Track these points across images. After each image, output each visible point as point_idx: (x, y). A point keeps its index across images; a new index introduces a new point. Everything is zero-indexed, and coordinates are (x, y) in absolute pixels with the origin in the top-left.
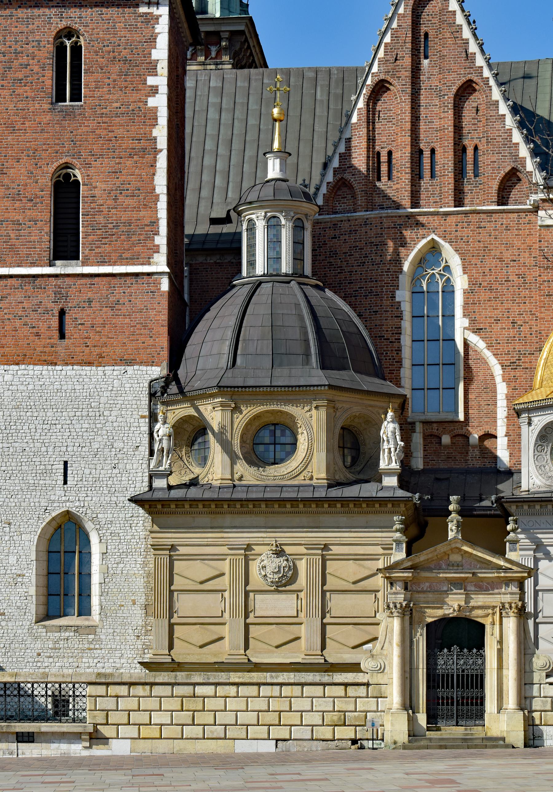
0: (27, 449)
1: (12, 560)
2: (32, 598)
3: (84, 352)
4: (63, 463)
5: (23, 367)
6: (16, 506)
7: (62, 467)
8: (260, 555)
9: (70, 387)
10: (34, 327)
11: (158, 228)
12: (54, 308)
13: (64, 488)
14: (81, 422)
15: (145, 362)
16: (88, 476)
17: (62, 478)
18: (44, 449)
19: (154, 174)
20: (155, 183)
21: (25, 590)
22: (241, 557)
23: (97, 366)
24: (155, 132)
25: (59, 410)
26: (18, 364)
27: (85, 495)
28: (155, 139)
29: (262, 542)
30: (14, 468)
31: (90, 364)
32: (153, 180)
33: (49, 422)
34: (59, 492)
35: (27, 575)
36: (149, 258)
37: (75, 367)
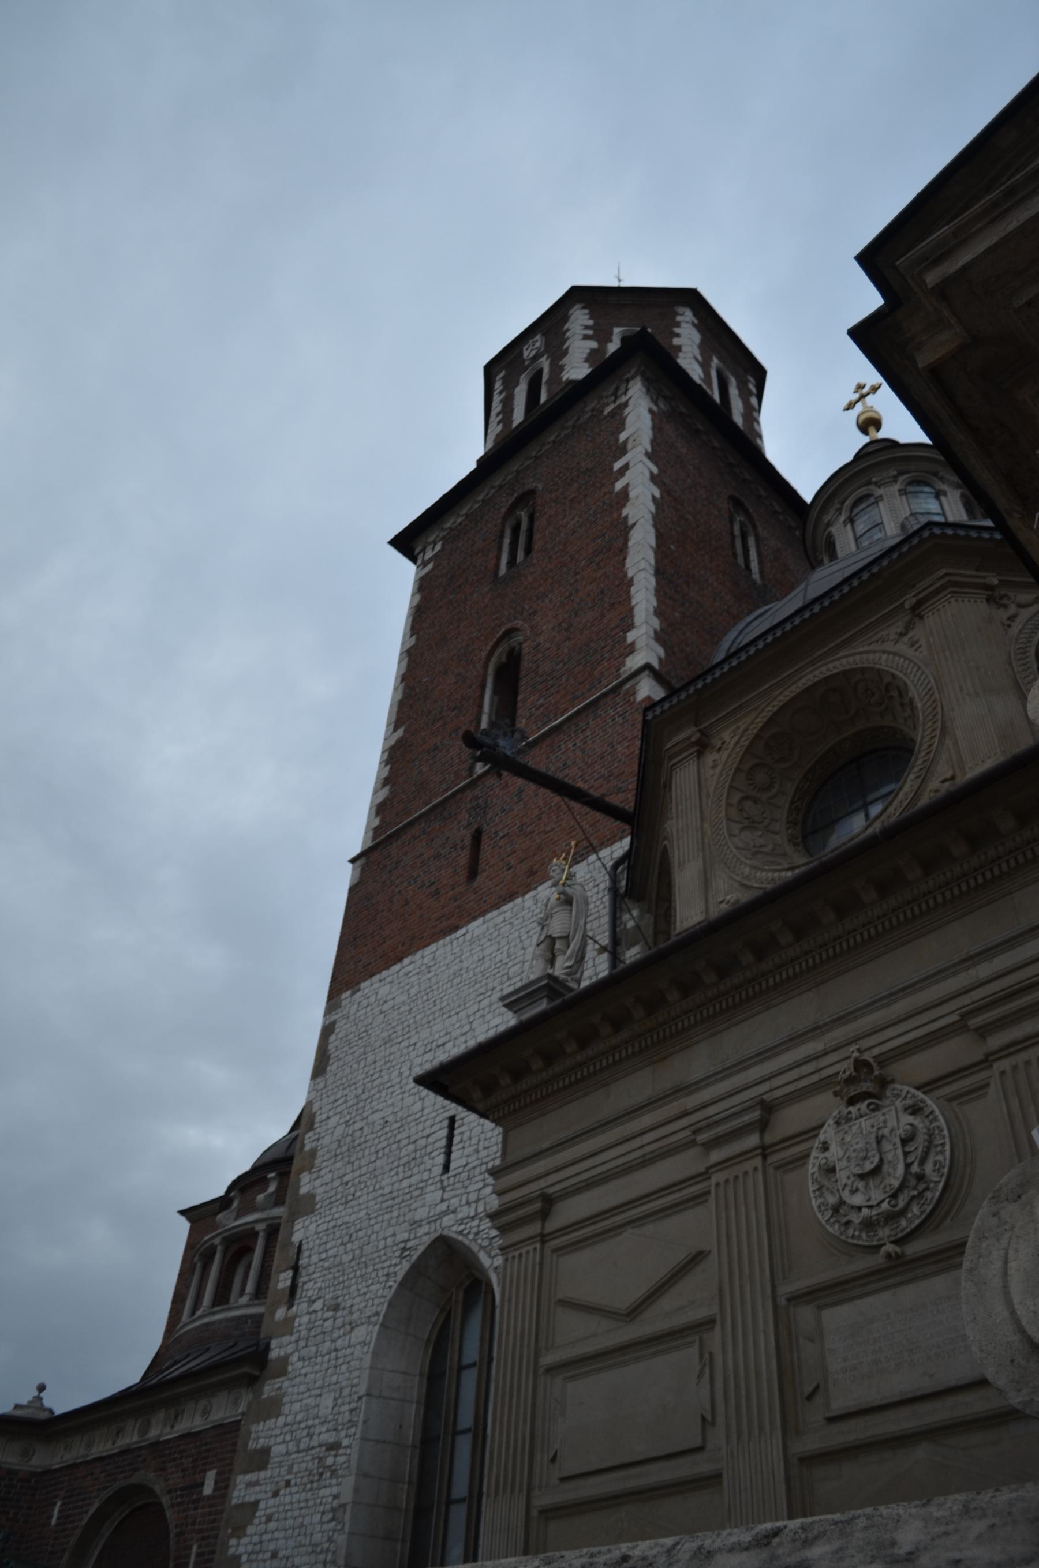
0: (391, 1119)
1: (327, 1401)
2: (345, 1512)
3: (503, 882)
4: (446, 1123)
5: (406, 961)
6: (353, 1259)
7: (444, 1132)
8: (813, 1131)
9: (475, 958)
10: (433, 883)
11: (632, 620)
12: (465, 835)
13: (442, 1181)
14: (489, 1017)
15: (608, 840)
16: (489, 1135)
17: (440, 1159)
18: (418, 1106)
19: (625, 558)
20: (627, 565)
21: (335, 1490)
22: (749, 1166)
23: (523, 895)
24: (625, 512)
25: (453, 1013)
26: (400, 960)
27: (481, 1184)
28: (626, 517)
29: (815, 1078)
30: (364, 1170)
31: (511, 896)
32: (623, 565)
33: (434, 1044)
34: (433, 1195)
35: (345, 1442)
36: (619, 670)
37: (489, 916)
